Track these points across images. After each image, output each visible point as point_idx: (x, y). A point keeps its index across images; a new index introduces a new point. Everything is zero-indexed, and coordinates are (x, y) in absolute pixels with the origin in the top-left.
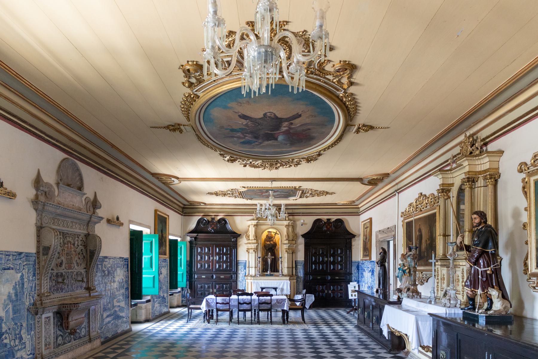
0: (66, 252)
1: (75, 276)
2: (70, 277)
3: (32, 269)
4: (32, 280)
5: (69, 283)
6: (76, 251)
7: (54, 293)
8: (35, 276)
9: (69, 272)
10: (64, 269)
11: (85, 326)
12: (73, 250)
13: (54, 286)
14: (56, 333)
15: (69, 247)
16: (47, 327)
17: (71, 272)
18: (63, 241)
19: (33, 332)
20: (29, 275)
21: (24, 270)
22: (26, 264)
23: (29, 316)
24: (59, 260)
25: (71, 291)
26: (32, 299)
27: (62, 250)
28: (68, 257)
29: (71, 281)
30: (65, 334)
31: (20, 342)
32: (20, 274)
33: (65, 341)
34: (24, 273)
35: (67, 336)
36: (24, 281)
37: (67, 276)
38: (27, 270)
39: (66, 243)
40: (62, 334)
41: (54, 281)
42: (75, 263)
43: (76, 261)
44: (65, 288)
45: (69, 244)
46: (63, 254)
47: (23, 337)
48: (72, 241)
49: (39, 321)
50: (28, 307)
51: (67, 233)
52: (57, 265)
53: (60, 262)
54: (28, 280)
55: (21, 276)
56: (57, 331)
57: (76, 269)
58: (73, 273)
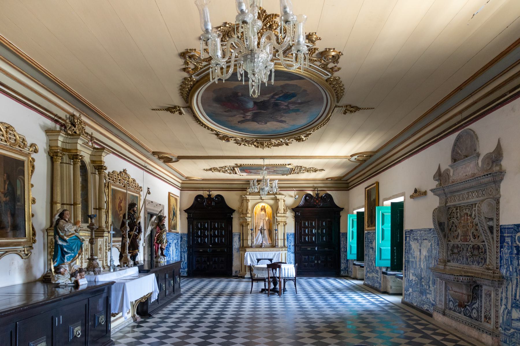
0: (462, 224)
2: (465, 249)
5: (464, 255)
6: (473, 222)
9: (464, 244)
10: (459, 242)
12: (469, 221)
15: (466, 219)
17: (466, 244)
25: (466, 264)
26: (436, 262)
27: (459, 223)
28: (464, 230)
29: (466, 253)
32: (430, 243)
37: (463, 249)
39: (463, 215)
42: (471, 235)
43: (473, 233)
45: (466, 216)
46: (460, 227)
48: (469, 213)
51: (463, 206)
52: (454, 237)
53: (457, 235)
57: (472, 242)
58: (469, 246)
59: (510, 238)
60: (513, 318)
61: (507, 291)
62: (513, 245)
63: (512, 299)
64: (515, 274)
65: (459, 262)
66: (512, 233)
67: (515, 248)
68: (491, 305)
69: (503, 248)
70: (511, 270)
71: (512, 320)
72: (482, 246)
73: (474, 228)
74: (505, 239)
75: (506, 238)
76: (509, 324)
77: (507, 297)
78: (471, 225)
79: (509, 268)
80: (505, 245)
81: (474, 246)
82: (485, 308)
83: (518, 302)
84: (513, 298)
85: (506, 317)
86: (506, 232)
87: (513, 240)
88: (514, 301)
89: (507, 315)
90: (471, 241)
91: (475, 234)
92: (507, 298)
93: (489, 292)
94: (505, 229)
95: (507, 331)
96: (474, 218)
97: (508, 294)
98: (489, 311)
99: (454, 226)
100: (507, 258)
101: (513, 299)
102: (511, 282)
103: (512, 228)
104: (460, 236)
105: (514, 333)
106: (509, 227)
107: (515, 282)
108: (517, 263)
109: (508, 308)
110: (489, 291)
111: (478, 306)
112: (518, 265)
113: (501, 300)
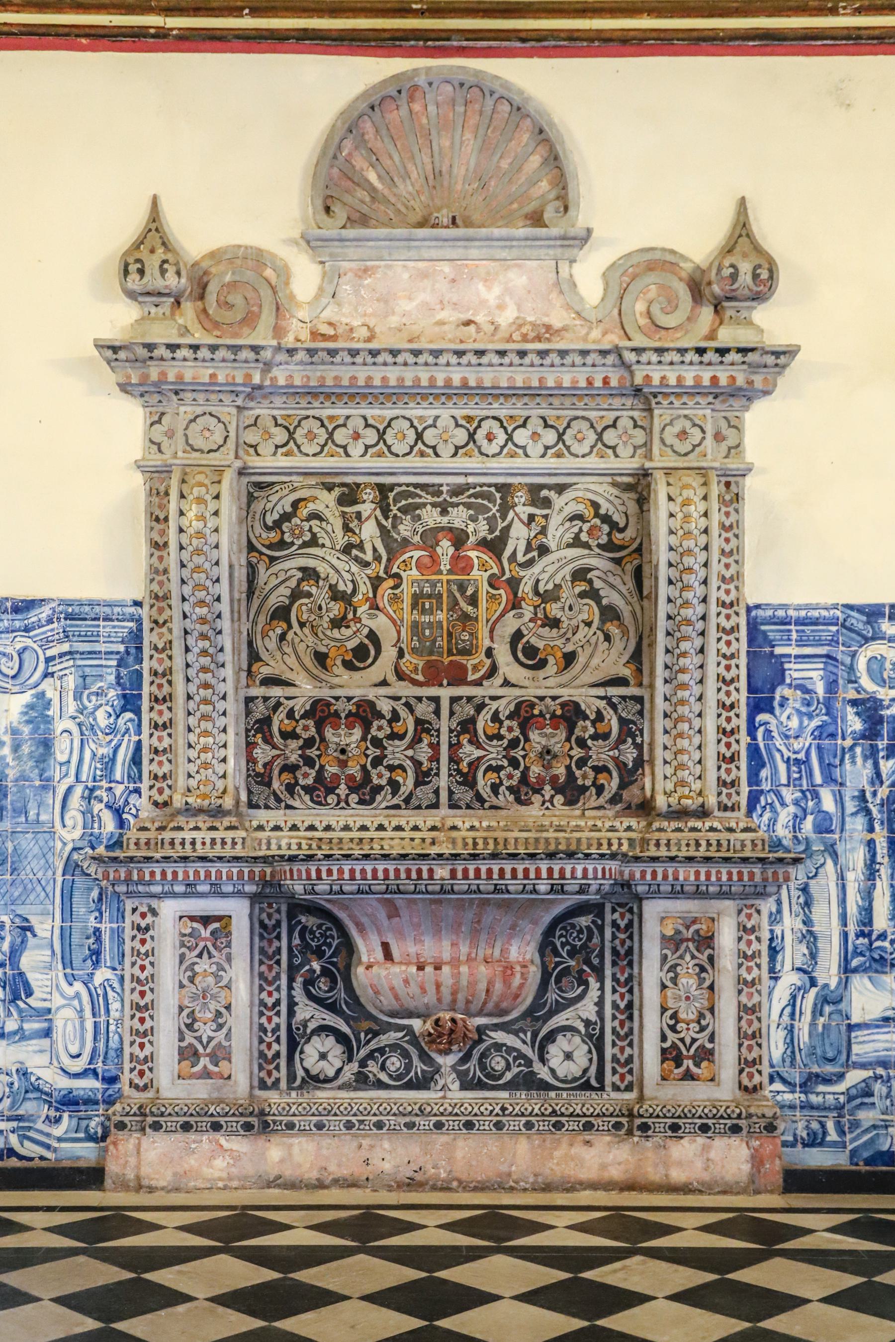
0: (407, 591)
1: (495, 718)
3: (112, 678)
4: (112, 730)
6: (514, 583)
7: (297, 803)
8: (138, 712)
9: (436, 700)
10: (384, 683)
11: (587, 1023)
13: (285, 768)
14: (291, 1013)
16: (203, 966)
17: (454, 700)
18: (384, 532)
19: (102, 975)
20: (90, 706)
21: (49, 680)
22: (61, 655)
23: (76, 894)
24: (347, 632)
25: (453, 806)
27: (376, 582)
30: (376, 1034)
31: (13, 1001)
32: (27, 697)
33: (373, 1067)
34: (49, 694)
35: (394, 1047)
36: (49, 731)
38: (71, 682)
40: (345, 1029)
41: (294, 744)
44: (395, 786)
47: (33, 984)
49: (147, 929)
50: (74, 849)
51: (416, 486)
54: (80, 725)
55: (31, 707)
56: (292, 1005)
57: (506, 683)
58: (480, 707)
59: (821, 666)
60: (855, 1020)
61: (808, 904)
62: (841, 695)
63: (845, 935)
64: (857, 824)
65: (384, 799)
66: (834, 642)
67: (850, 710)
68: (711, 988)
69: (771, 711)
70: (828, 803)
71: (851, 1028)
72: (602, 704)
73: (528, 611)
74: (784, 670)
75: (787, 666)
76: (830, 1055)
77: (810, 932)
78: (492, 598)
79: (816, 796)
80: (784, 699)
81: (532, 706)
82: (664, 1010)
83: (886, 944)
84: (852, 928)
85: (813, 1024)
86: (794, 636)
87: (842, 674)
88: (861, 940)
89: (817, 1012)
90: (499, 681)
91: (540, 644)
92: (810, 937)
93: (696, 927)
94: (789, 623)
95: (821, 1088)
96: (521, 558)
97: (815, 917)
98: (701, 1016)
99: (320, 594)
100: (801, 756)
101: (851, 936)
102: (830, 863)
103: (834, 622)
104: (389, 654)
105: (867, 1086)
106: (815, 614)
107: (857, 857)
108: (867, 771)
109: (821, 982)
110: (695, 921)
111: (600, 1014)
112: (872, 783)
113: (774, 952)
